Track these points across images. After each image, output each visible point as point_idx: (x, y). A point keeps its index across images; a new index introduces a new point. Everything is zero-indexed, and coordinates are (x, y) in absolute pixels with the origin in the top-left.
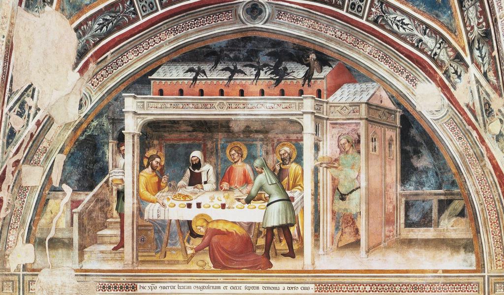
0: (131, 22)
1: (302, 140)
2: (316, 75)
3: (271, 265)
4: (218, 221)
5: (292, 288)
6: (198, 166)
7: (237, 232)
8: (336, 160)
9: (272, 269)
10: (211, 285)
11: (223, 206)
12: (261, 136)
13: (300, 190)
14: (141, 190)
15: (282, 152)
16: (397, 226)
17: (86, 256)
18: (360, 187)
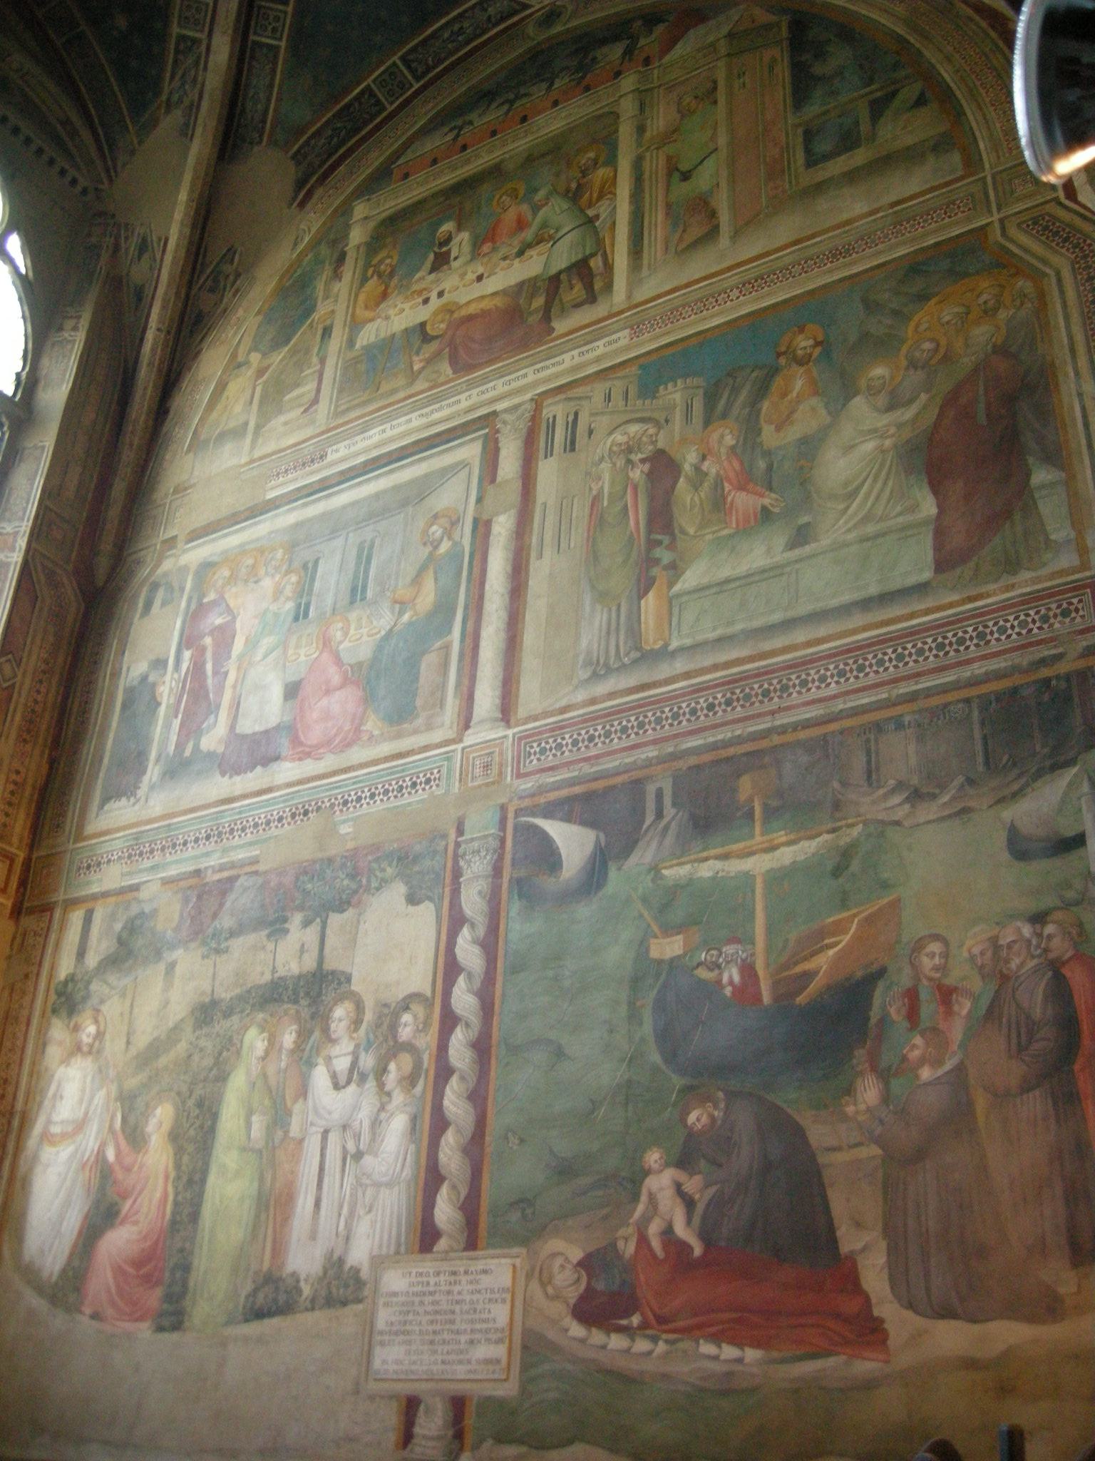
0: (379, 112)
1: (616, 131)
2: (642, 42)
3: (554, 329)
4: (469, 303)
5: (588, 351)
6: (448, 240)
7: (499, 304)
8: (675, 131)
9: (554, 335)
10: (443, 403)
11: (480, 278)
12: (549, 158)
13: (611, 199)
14: (358, 311)
15: (583, 162)
16: (790, 175)
17: (260, 440)
18: (716, 149)
